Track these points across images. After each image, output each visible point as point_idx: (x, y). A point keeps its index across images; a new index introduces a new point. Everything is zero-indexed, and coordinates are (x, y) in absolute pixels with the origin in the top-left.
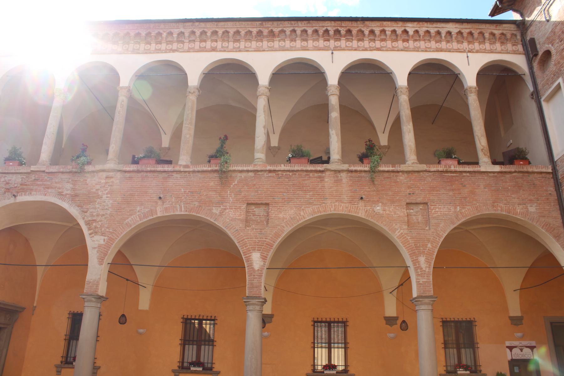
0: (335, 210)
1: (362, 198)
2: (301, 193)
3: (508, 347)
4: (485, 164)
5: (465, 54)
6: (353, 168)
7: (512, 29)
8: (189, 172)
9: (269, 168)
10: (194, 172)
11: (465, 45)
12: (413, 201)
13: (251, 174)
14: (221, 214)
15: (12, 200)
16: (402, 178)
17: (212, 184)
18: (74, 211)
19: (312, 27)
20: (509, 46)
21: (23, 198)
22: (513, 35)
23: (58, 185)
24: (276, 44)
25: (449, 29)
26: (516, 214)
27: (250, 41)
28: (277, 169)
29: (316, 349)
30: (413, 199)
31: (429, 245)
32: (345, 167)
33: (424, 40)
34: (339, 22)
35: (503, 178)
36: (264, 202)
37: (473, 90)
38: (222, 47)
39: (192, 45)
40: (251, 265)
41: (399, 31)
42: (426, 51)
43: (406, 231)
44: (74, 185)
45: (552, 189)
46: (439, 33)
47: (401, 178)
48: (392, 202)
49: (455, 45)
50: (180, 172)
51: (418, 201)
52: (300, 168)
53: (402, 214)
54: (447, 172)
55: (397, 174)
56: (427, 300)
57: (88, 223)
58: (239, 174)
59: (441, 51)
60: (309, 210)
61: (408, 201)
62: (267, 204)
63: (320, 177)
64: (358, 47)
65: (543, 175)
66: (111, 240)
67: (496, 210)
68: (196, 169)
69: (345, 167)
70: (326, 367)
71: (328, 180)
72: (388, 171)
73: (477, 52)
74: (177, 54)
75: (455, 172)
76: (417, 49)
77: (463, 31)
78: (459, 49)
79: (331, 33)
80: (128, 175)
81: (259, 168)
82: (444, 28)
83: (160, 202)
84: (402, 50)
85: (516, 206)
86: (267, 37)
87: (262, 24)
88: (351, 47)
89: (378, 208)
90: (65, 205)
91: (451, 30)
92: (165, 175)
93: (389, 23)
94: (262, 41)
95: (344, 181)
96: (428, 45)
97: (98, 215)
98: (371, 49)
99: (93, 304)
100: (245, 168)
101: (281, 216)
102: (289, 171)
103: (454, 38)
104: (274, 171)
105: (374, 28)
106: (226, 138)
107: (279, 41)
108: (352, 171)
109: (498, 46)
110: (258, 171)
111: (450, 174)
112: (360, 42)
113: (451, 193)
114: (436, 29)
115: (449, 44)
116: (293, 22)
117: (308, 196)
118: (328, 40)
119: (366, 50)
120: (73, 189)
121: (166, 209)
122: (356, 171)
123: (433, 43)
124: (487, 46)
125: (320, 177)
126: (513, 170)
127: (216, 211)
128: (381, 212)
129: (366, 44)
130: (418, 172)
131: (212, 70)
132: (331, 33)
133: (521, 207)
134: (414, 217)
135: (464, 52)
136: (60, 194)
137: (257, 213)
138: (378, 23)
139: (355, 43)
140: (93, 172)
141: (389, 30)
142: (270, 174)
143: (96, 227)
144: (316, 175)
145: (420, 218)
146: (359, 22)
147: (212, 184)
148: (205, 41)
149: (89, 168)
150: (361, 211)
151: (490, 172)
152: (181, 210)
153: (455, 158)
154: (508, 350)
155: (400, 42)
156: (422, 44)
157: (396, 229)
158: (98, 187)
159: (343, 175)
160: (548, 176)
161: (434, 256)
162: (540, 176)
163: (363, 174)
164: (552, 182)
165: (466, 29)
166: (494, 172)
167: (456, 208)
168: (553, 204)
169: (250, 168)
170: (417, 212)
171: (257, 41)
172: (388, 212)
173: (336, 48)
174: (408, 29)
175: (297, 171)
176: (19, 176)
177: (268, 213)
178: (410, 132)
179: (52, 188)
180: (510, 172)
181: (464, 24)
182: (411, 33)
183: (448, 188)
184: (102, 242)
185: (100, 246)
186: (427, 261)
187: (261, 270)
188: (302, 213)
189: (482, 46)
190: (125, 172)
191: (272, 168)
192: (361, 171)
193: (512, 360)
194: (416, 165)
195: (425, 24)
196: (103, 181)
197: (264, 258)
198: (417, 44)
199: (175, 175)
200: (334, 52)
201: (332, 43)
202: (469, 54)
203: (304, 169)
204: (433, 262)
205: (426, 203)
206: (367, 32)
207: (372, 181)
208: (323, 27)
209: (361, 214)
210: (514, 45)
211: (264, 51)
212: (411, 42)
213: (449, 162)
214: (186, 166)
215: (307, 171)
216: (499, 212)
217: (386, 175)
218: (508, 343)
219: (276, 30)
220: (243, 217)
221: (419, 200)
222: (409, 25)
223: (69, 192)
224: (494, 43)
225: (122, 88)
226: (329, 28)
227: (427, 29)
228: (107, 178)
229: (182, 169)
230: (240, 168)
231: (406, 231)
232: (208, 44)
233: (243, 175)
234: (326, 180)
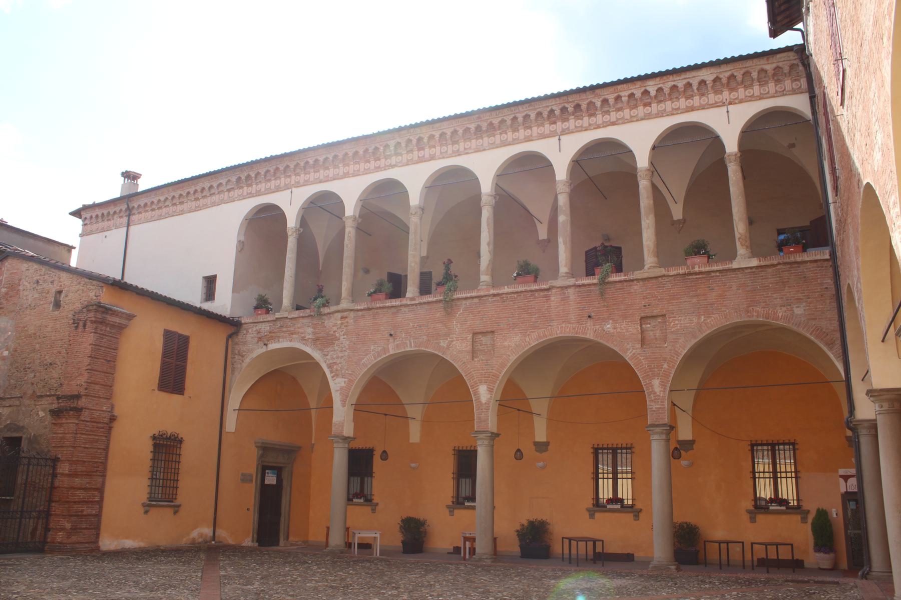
0: (561, 333)
1: (589, 317)
2: (526, 316)
3: (841, 476)
4: (744, 259)
5: (724, 109)
6: (580, 282)
7: (792, 58)
8: (416, 305)
9: (492, 292)
10: (420, 304)
11: (726, 94)
12: (649, 315)
13: (476, 300)
14: (448, 347)
15: (264, 349)
16: (636, 287)
17: (438, 315)
18: (316, 355)
19: (535, 109)
20: (788, 84)
21: (273, 346)
22: (792, 67)
23: (301, 330)
24: (498, 139)
25: (702, 78)
26: (777, 319)
27: (470, 139)
28: (500, 292)
29: (601, 481)
30: (648, 312)
31: (665, 366)
32: (572, 281)
33: (671, 99)
34: (565, 98)
35: (763, 274)
36: (489, 330)
37: (733, 158)
38: (441, 153)
39: (410, 156)
40: (478, 399)
41: (638, 93)
42: (673, 114)
43: (639, 351)
44: (314, 328)
45: (829, 281)
46: (689, 85)
47: (636, 287)
48: (624, 317)
49: (712, 98)
50: (408, 305)
51: (654, 314)
52: (523, 289)
53: (635, 331)
54: (690, 274)
55: (631, 283)
56: (658, 429)
57: (330, 366)
58: (464, 302)
59: (692, 110)
60: (534, 335)
61: (643, 315)
62: (493, 332)
63: (546, 296)
64: (590, 125)
65: (819, 263)
66: (351, 381)
67: (749, 317)
68: (422, 301)
69: (572, 281)
70: (609, 501)
71: (555, 298)
72: (620, 281)
73: (741, 102)
74: (396, 169)
75: (700, 273)
76: (660, 115)
77: (721, 76)
78: (716, 103)
79: (557, 112)
80: (360, 313)
81: (482, 293)
82: (695, 78)
83: (391, 339)
84: (642, 119)
85: (778, 308)
86: (487, 131)
87: (479, 118)
88: (581, 126)
89: (608, 327)
90: (308, 350)
91: (705, 78)
92: (394, 310)
93: (624, 86)
94: (482, 138)
95: (572, 297)
96: (676, 105)
97: (338, 357)
98: (605, 125)
99: (341, 445)
100: (469, 295)
101: (506, 344)
102: (513, 293)
103: (709, 89)
104: (498, 295)
105: (606, 97)
106: (450, 261)
107: (501, 134)
108: (579, 286)
109: (771, 87)
110: (482, 297)
111: (695, 277)
112: (593, 118)
113: (694, 300)
114: (685, 82)
115: (704, 98)
116: (513, 108)
117: (533, 320)
118: (555, 123)
119: (598, 127)
120: (314, 333)
121: (398, 346)
122: (584, 285)
123: (682, 100)
124: (756, 90)
125: (546, 296)
126: (775, 262)
127: (443, 344)
128: (612, 330)
129: (599, 119)
130: (656, 278)
131: (434, 181)
132: (557, 112)
133: (784, 309)
134: (651, 333)
135: (724, 104)
136: (303, 340)
137: (484, 342)
138: (611, 89)
139: (586, 121)
140: (329, 314)
141: (625, 94)
142: (495, 299)
143: (337, 370)
144: (542, 294)
145: (658, 333)
146: (588, 93)
147: (438, 315)
148: (423, 149)
149: (325, 310)
150: (589, 332)
151: (746, 268)
152: (411, 346)
153: (704, 254)
154: (842, 481)
155: (641, 108)
156: (668, 105)
157: (628, 350)
158: (335, 329)
159: (571, 291)
160: (825, 264)
161: (671, 378)
162: (815, 265)
163: (593, 288)
164: (830, 271)
165: (724, 73)
166: (751, 268)
167: (699, 318)
168: (828, 301)
169: (474, 294)
170: (655, 326)
171: (477, 139)
172: (619, 330)
173: (565, 132)
174: (649, 89)
175: (521, 292)
176: (268, 324)
177: (494, 341)
178: (648, 228)
179: (295, 333)
180: (773, 265)
181: (722, 66)
182: (653, 93)
183: (691, 294)
184: (343, 385)
185: (342, 388)
186: (662, 385)
187: (487, 403)
188: (527, 339)
189: (749, 92)
190: (358, 310)
191: (495, 292)
192: (589, 285)
193: (847, 493)
194: (655, 270)
195: (671, 78)
196: (339, 322)
197: (490, 390)
198: (662, 106)
199: (403, 309)
200: (562, 137)
201: (559, 126)
202: (731, 107)
203: (528, 289)
204: (668, 386)
205: (664, 316)
206: (598, 104)
207: (602, 294)
208: (547, 107)
209: (590, 335)
210: (796, 80)
211: (484, 150)
212: (654, 105)
213: (697, 260)
214: (413, 299)
215: (532, 291)
216: (754, 318)
217: (618, 286)
218: (842, 472)
219: (496, 121)
220: (469, 348)
221: (655, 312)
222: (650, 83)
223: (310, 337)
224: (766, 83)
225: (348, 217)
226: (554, 108)
227: (673, 83)
228: (342, 318)
229: (409, 303)
230: (464, 296)
231: (639, 351)
232: (427, 152)
233: (468, 302)
234: (552, 298)
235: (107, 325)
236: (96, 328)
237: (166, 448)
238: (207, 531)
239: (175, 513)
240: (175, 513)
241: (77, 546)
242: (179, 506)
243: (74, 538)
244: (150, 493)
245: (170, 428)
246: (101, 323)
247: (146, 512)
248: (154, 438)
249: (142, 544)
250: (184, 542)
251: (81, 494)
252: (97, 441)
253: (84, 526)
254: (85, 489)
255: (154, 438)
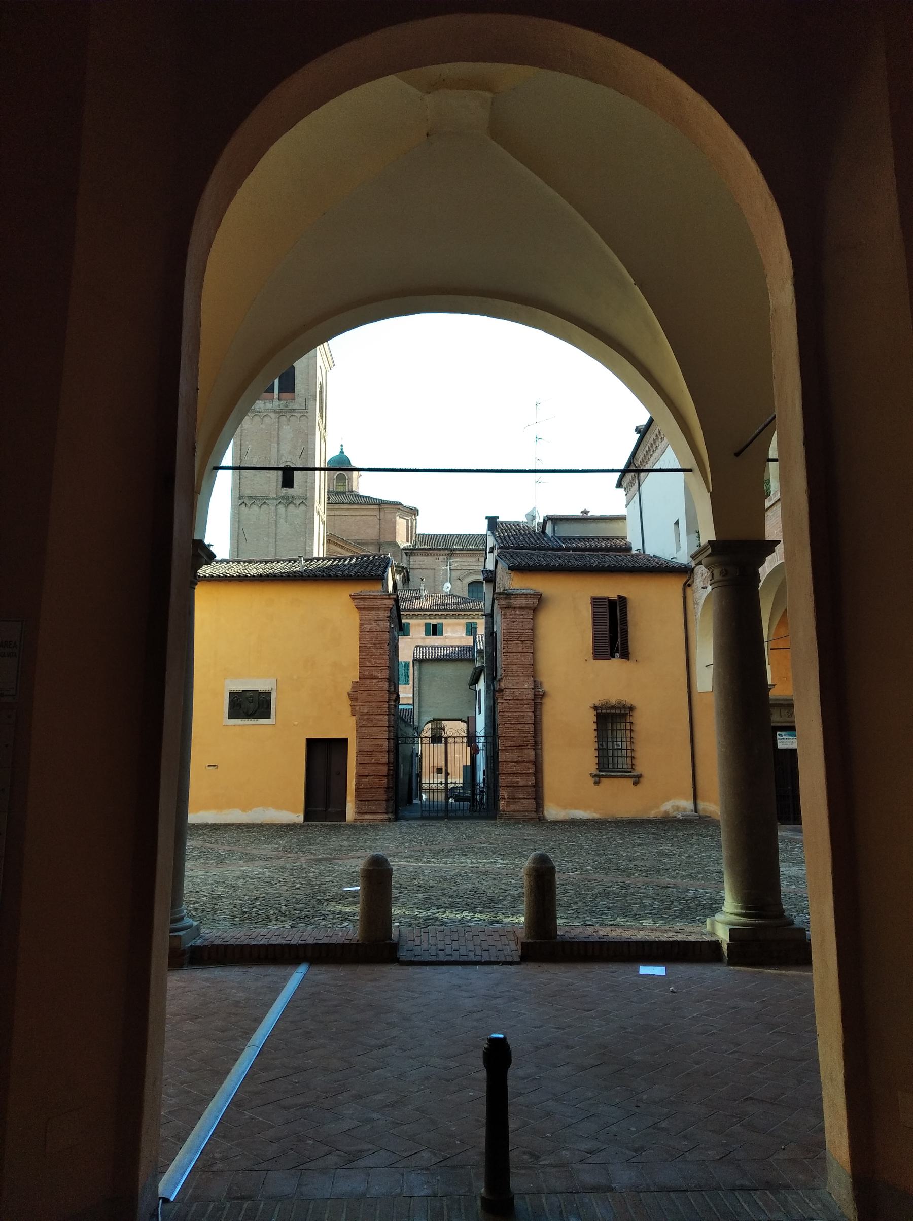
235: (515, 608)
236: (505, 614)
237: (612, 719)
238: (688, 805)
239: (635, 783)
240: (635, 783)
241: (517, 814)
242: (639, 777)
243: (512, 807)
244: (598, 764)
245: (614, 695)
246: (508, 608)
247: (596, 783)
248: (595, 708)
249: (596, 816)
250: (652, 814)
251: (514, 767)
252: (523, 717)
253: (521, 796)
254: (517, 762)
255: (595, 708)
